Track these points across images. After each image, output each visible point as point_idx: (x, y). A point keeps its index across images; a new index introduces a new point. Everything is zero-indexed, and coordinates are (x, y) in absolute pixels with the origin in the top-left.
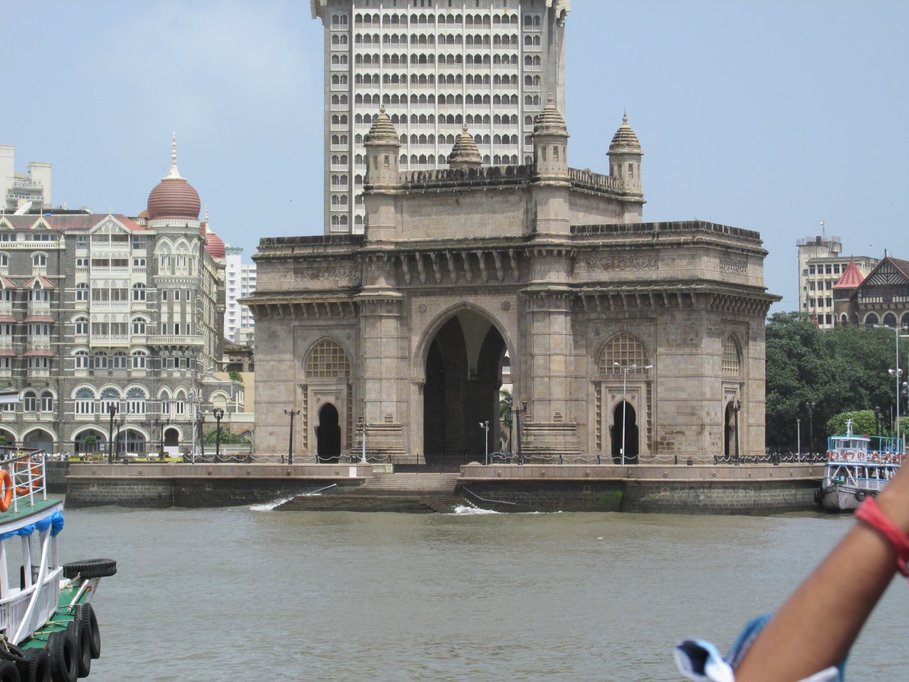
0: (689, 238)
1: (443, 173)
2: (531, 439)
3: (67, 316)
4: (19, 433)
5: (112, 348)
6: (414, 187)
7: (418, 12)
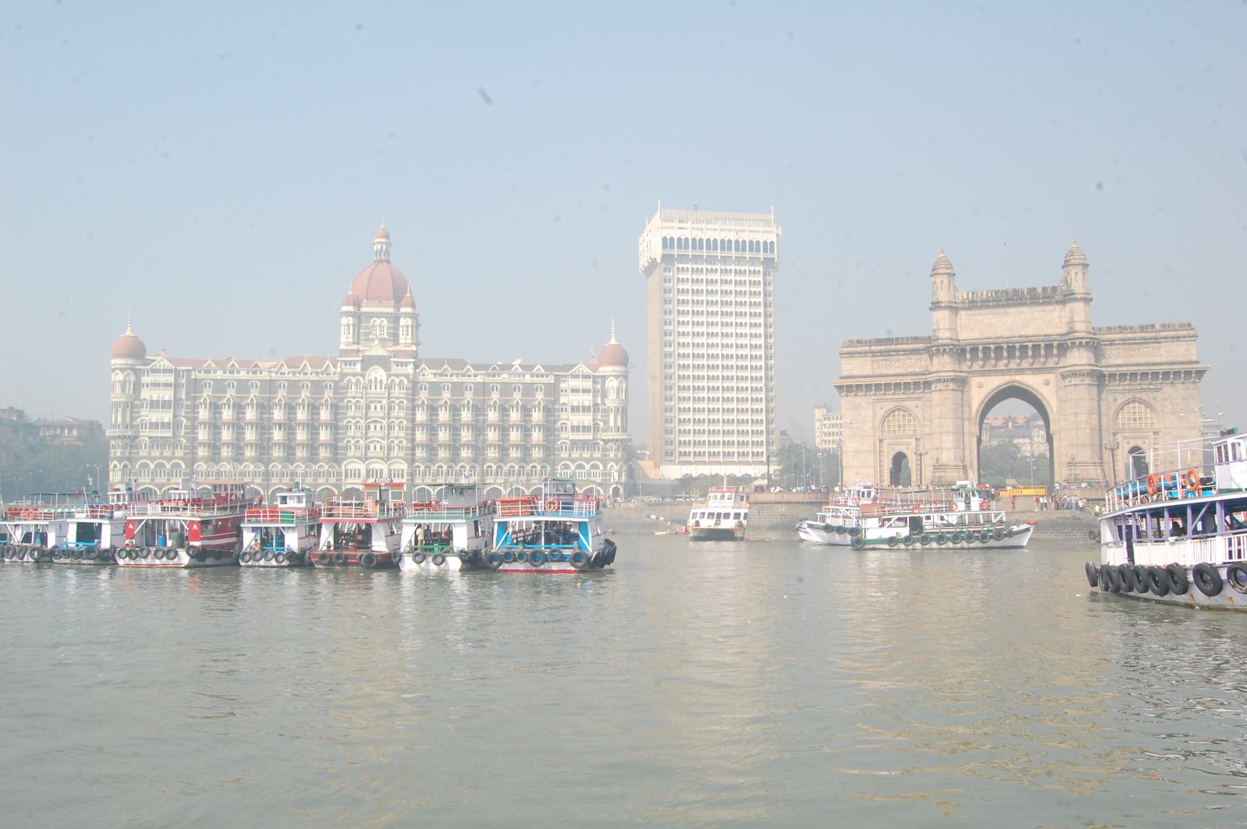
0: (1184, 333)
1: (992, 292)
2: (1079, 472)
3: (555, 422)
4: (528, 490)
5: (582, 440)
6: (969, 302)
7: (709, 267)
